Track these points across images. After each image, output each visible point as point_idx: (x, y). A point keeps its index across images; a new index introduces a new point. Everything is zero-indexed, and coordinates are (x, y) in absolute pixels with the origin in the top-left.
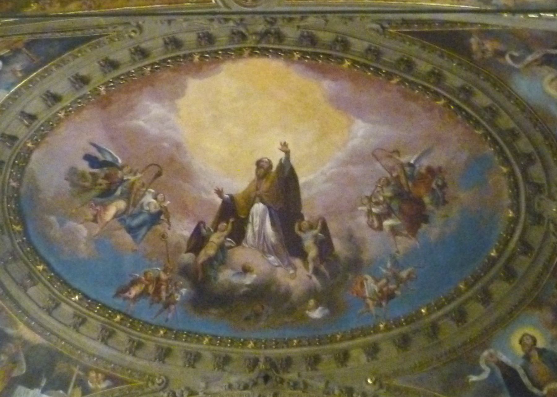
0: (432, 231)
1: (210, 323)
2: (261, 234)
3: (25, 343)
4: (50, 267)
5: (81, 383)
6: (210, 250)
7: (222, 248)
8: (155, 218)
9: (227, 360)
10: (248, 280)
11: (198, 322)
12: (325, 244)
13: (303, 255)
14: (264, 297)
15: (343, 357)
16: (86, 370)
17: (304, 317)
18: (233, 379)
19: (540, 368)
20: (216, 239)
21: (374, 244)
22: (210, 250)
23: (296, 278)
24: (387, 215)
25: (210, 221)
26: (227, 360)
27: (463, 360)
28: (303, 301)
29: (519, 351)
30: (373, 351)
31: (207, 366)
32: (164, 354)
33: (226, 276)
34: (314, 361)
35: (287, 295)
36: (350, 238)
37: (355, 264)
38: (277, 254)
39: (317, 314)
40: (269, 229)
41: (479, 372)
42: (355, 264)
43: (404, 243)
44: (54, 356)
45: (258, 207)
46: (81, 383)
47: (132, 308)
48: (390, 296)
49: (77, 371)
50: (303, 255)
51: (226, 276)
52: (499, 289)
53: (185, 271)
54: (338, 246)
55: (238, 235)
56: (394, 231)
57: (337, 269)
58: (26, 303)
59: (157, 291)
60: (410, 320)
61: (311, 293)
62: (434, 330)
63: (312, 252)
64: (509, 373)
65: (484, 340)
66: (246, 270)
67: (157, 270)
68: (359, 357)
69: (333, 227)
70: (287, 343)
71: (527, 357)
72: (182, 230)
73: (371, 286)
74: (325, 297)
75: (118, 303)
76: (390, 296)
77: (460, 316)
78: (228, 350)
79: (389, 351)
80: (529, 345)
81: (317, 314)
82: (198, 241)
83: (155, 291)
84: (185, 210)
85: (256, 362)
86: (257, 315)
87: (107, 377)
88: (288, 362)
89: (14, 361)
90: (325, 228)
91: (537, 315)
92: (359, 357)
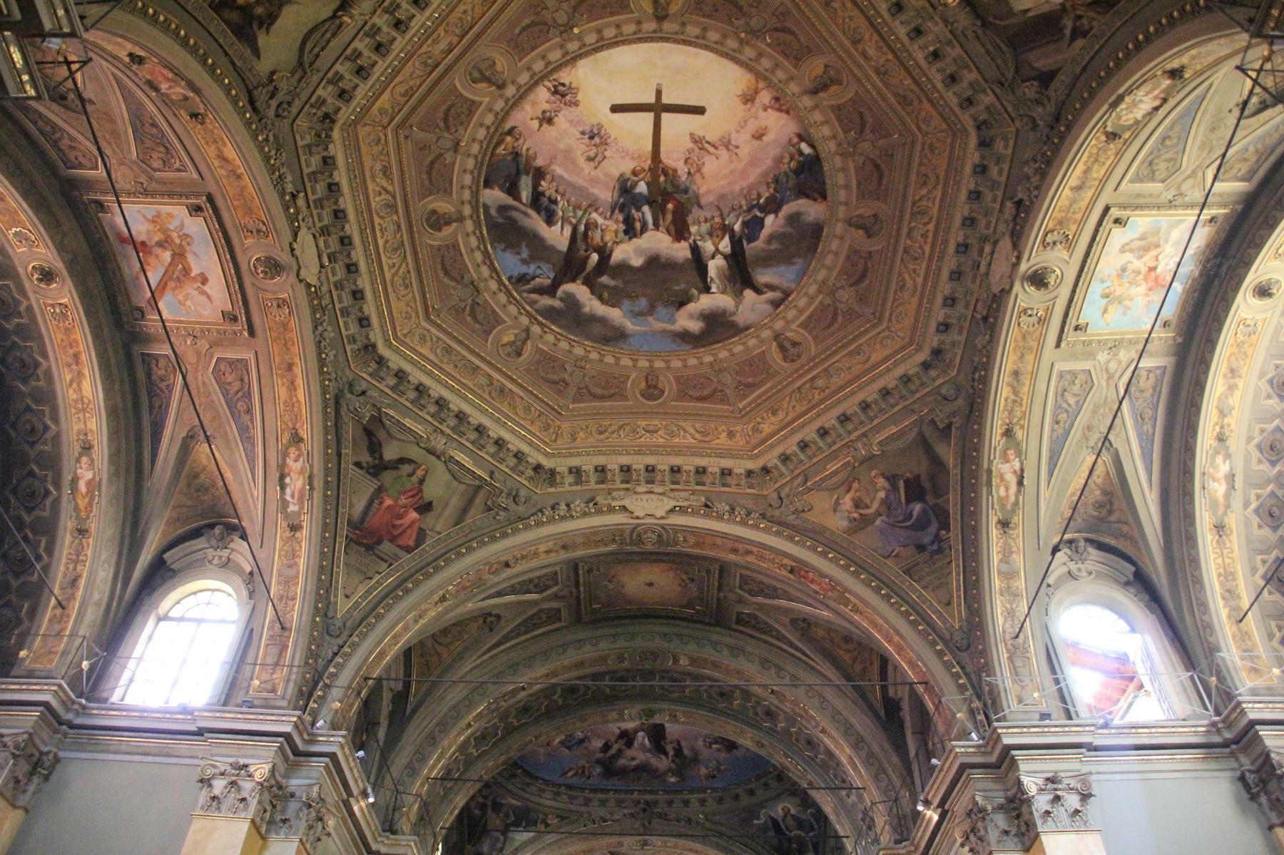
0: (738, 753)
1: (614, 782)
2: (643, 744)
3: (512, 806)
4: (525, 771)
5: (544, 821)
6: (613, 751)
7: (620, 751)
8: (582, 741)
9: (622, 801)
10: (634, 763)
11: (606, 783)
12: (679, 751)
13: (666, 754)
14: (643, 768)
15: (686, 803)
16: (546, 815)
17: (665, 781)
18: (626, 811)
19: (791, 823)
20: (616, 747)
21: (705, 753)
22: (613, 751)
23: (662, 763)
24: (716, 742)
25: (613, 739)
26: (622, 801)
27: (752, 813)
28: (665, 773)
29: (781, 812)
30: (703, 802)
31: (612, 803)
32: (587, 802)
33: (622, 762)
34: (670, 803)
35: (656, 770)
36: (693, 749)
37: (696, 760)
38: (649, 751)
39: (673, 780)
40: (647, 741)
41: (758, 819)
42: (696, 760)
43: (723, 755)
44: (528, 810)
45: (641, 734)
46: (544, 821)
47: (570, 782)
48: (714, 777)
49: (541, 816)
50: (666, 754)
51: (622, 762)
52: (773, 784)
53: (598, 762)
54: (686, 751)
55: (629, 744)
56: (718, 750)
57: (684, 762)
58: (510, 787)
59: (583, 772)
60: (724, 789)
61: (670, 770)
62: (736, 797)
63: (671, 753)
64: (775, 822)
65: (762, 805)
66: (633, 759)
67: (583, 762)
68: (695, 803)
69: (683, 744)
70: (656, 792)
71: (785, 816)
72: (598, 744)
73: (703, 771)
74: (679, 772)
75: (562, 780)
76: (714, 777)
77: (751, 792)
78: (623, 796)
79: (712, 805)
80: (787, 812)
81: (673, 780)
82: (607, 747)
83: (582, 772)
84: (599, 737)
85: (639, 802)
86: (639, 779)
87: (557, 816)
88: (656, 802)
89: (507, 816)
90: (679, 743)
91: (791, 799)
92: (695, 803)
